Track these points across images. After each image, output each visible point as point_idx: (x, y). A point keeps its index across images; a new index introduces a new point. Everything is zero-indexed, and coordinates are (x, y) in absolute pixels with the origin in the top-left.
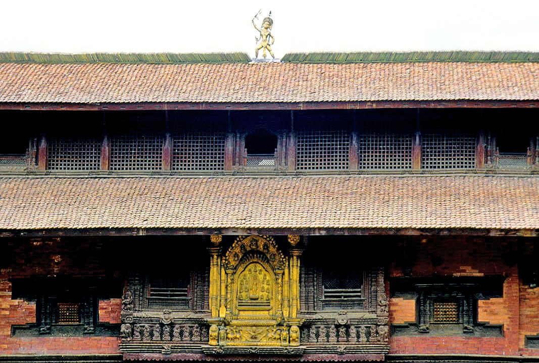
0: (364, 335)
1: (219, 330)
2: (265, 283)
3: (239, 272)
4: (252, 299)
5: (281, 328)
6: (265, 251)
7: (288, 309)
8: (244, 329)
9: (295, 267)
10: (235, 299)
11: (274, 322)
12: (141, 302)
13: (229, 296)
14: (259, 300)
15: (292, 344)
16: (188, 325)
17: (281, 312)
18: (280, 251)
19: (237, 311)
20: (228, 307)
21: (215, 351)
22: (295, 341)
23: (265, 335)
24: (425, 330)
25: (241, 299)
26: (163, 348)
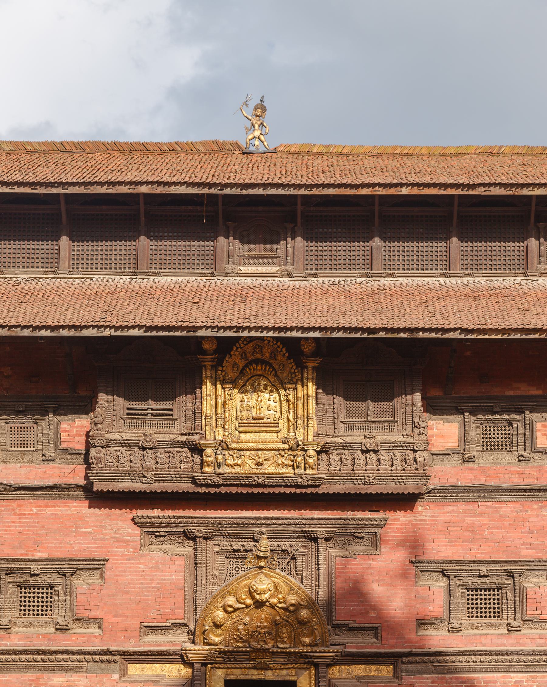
2: (272, 400)
4: (254, 419)
11: (285, 446)
13: (227, 414)
15: (309, 471)
16: (175, 449)
17: (293, 434)
18: (292, 361)
19: (237, 433)
21: (211, 480)
22: (313, 469)
24: (472, 458)
25: (242, 419)
26: (146, 477)
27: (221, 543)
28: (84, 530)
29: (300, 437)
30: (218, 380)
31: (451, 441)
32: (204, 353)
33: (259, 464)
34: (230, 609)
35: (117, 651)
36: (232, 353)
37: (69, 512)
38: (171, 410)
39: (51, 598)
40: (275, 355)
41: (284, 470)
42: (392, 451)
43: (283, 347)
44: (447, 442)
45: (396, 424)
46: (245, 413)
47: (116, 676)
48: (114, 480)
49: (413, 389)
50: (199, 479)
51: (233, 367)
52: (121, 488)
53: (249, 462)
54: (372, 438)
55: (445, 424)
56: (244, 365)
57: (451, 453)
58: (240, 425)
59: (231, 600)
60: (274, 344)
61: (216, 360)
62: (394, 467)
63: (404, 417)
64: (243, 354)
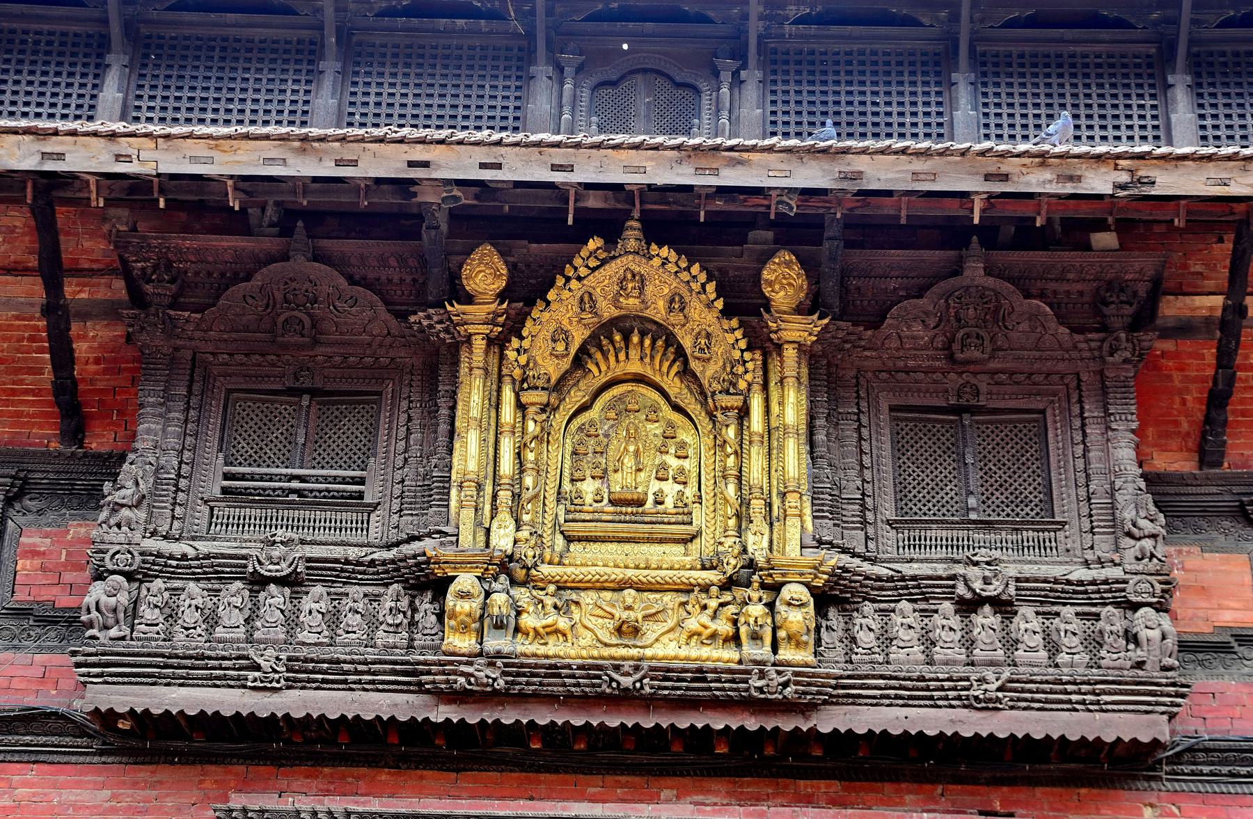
0: (1075, 641)
1: (488, 594)
2: (672, 451)
3: (571, 404)
5: (740, 593)
6: (676, 318)
7: (766, 530)
9: (791, 382)
10: (551, 499)
12: (178, 510)
13: (529, 481)
15: (786, 654)
19: (560, 541)
20: (526, 518)
21: (467, 675)
22: (799, 645)
23: (671, 623)
25: (576, 501)
26: (258, 668)
29: (757, 544)
30: (507, 379)
31: (1233, 604)
32: (469, 299)
36: (551, 296)
38: (362, 481)
41: (705, 652)
42: (1055, 608)
43: (709, 280)
44: (1221, 607)
45: (1060, 535)
46: (589, 488)
48: (154, 680)
49: (1108, 428)
50: (429, 673)
51: (554, 341)
52: (175, 704)
54: (988, 563)
55: (1206, 555)
56: (587, 333)
57: (1235, 644)
58: (571, 517)
60: (680, 270)
61: (501, 320)
62: (1063, 658)
63: (1085, 511)
64: (586, 298)
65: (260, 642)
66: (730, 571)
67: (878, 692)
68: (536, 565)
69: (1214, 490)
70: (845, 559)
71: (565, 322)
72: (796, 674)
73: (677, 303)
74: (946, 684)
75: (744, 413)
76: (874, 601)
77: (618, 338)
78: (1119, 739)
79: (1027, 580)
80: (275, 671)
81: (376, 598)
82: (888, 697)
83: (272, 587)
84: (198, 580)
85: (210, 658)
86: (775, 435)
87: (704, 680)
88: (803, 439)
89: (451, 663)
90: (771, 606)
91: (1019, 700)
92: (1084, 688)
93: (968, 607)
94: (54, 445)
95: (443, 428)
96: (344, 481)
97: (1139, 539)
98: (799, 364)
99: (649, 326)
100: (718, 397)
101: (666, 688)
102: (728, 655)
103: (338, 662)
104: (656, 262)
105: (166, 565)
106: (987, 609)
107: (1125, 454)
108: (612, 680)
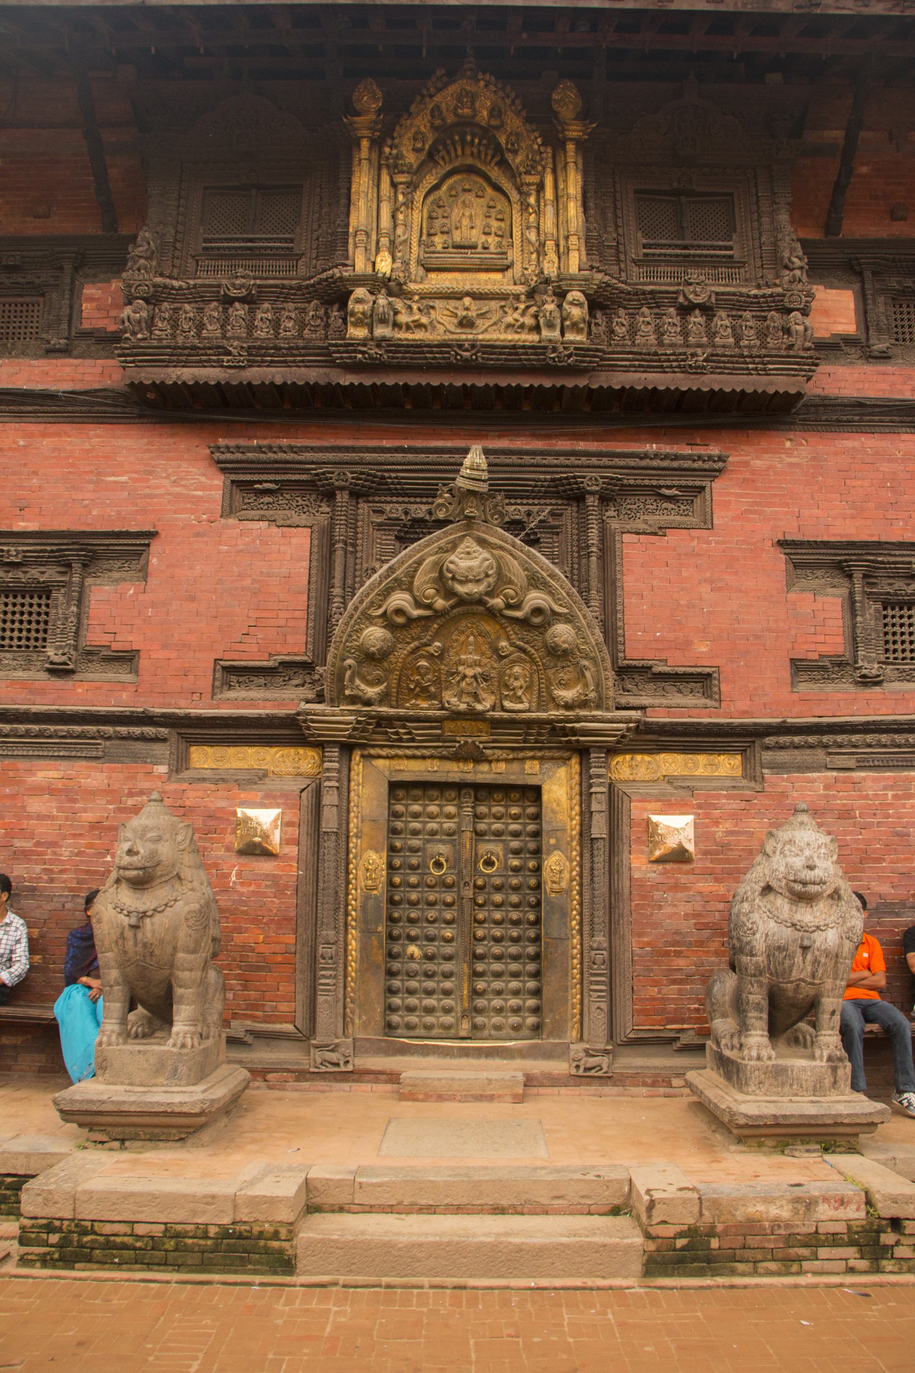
0: (752, 332)
2: (493, 215)
7: (556, 260)
8: (438, 304)
9: (571, 165)
10: (415, 245)
13: (400, 231)
14: (479, 249)
15: (569, 337)
19: (421, 271)
20: (399, 255)
21: (363, 353)
22: (579, 331)
23: (494, 320)
26: (230, 354)
27: (388, 507)
28: (113, 478)
29: (550, 268)
33: (466, 323)
34: (400, 620)
35: (164, 715)
36: (413, 108)
37: (87, 446)
38: (292, 241)
39: (47, 614)
40: (500, 111)
41: (517, 337)
44: (835, 322)
45: (742, 271)
47: (163, 769)
51: (415, 139)
52: (178, 377)
53: (445, 320)
59: (400, 599)
62: (744, 343)
65: (231, 338)
66: (533, 284)
67: (628, 363)
68: (405, 283)
69: (833, 251)
70: (607, 278)
71: (422, 128)
72: (576, 349)
73: (495, 112)
74: (672, 358)
75: (541, 187)
76: (625, 308)
77: (457, 138)
78: (777, 392)
79: (723, 294)
80: (240, 355)
81: (303, 311)
82: (634, 366)
83: (237, 305)
84: (189, 303)
85: (200, 348)
86: (561, 201)
87: (517, 354)
88: (579, 203)
89: (352, 345)
90: (560, 306)
91: (717, 368)
92: (757, 360)
93: (686, 310)
94: (100, 233)
95: (343, 201)
96: (280, 240)
97: (792, 270)
98: (576, 153)
99: (477, 130)
100: (523, 176)
101: (492, 359)
102: (531, 338)
103: (280, 349)
104: (482, 84)
105: (170, 294)
106: (697, 312)
107: (784, 217)
108: (457, 354)
